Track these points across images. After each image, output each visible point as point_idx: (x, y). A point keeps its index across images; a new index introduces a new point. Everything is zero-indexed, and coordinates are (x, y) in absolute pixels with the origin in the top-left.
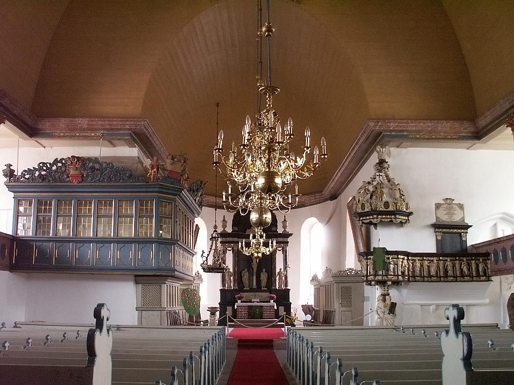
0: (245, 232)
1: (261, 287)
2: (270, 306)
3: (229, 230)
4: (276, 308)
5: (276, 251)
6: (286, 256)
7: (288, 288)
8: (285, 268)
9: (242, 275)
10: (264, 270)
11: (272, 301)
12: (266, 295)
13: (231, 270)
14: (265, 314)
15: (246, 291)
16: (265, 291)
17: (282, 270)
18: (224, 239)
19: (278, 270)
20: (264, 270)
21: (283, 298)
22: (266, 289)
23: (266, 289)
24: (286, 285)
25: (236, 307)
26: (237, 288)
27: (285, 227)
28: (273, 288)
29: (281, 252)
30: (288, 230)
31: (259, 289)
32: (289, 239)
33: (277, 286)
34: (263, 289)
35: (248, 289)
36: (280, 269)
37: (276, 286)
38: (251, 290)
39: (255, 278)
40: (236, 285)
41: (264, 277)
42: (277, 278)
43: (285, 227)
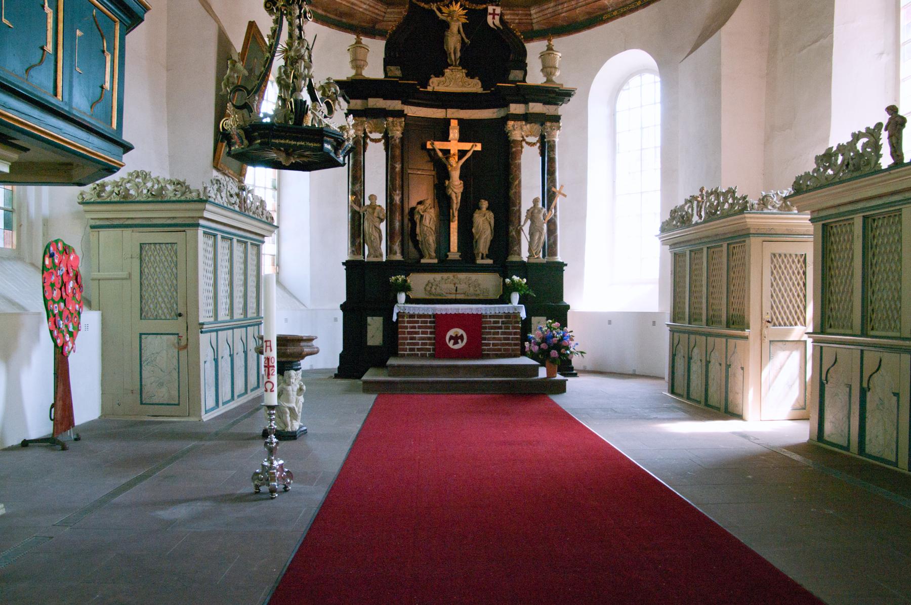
0: (425, 85)
1: (473, 259)
2: (508, 316)
3: (374, 70)
4: (523, 315)
5: (522, 147)
6: (552, 161)
7: (559, 258)
8: (549, 196)
9: (417, 217)
10: (485, 204)
11: (515, 297)
12: (488, 282)
13: (381, 201)
14: (490, 342)
15: (429, 269)
16: (484, 269)
17: (540, 205)
18: (357, 104)
19: (526, 204)
20: (485, 204)
21: (545, 287)
22: (490, 261)
23: (490, 261)
24: (551, 248)
25: (395, 318)
26: (398, 257)
27: (548, 69)
28: (513, 258)
29: (536, 150)
30: (562, 79)
31: (467, 262)
32: (563, 110)
33: (525, 255)
34: (479, 261)
35: (436, 261)
36: (535, 201)
37: (519, 254)
38: (444, 265)
39: (454, 226)
40: (397, 247)
41: (484, 222)
42: (526, 228)
43: (548, 69)
